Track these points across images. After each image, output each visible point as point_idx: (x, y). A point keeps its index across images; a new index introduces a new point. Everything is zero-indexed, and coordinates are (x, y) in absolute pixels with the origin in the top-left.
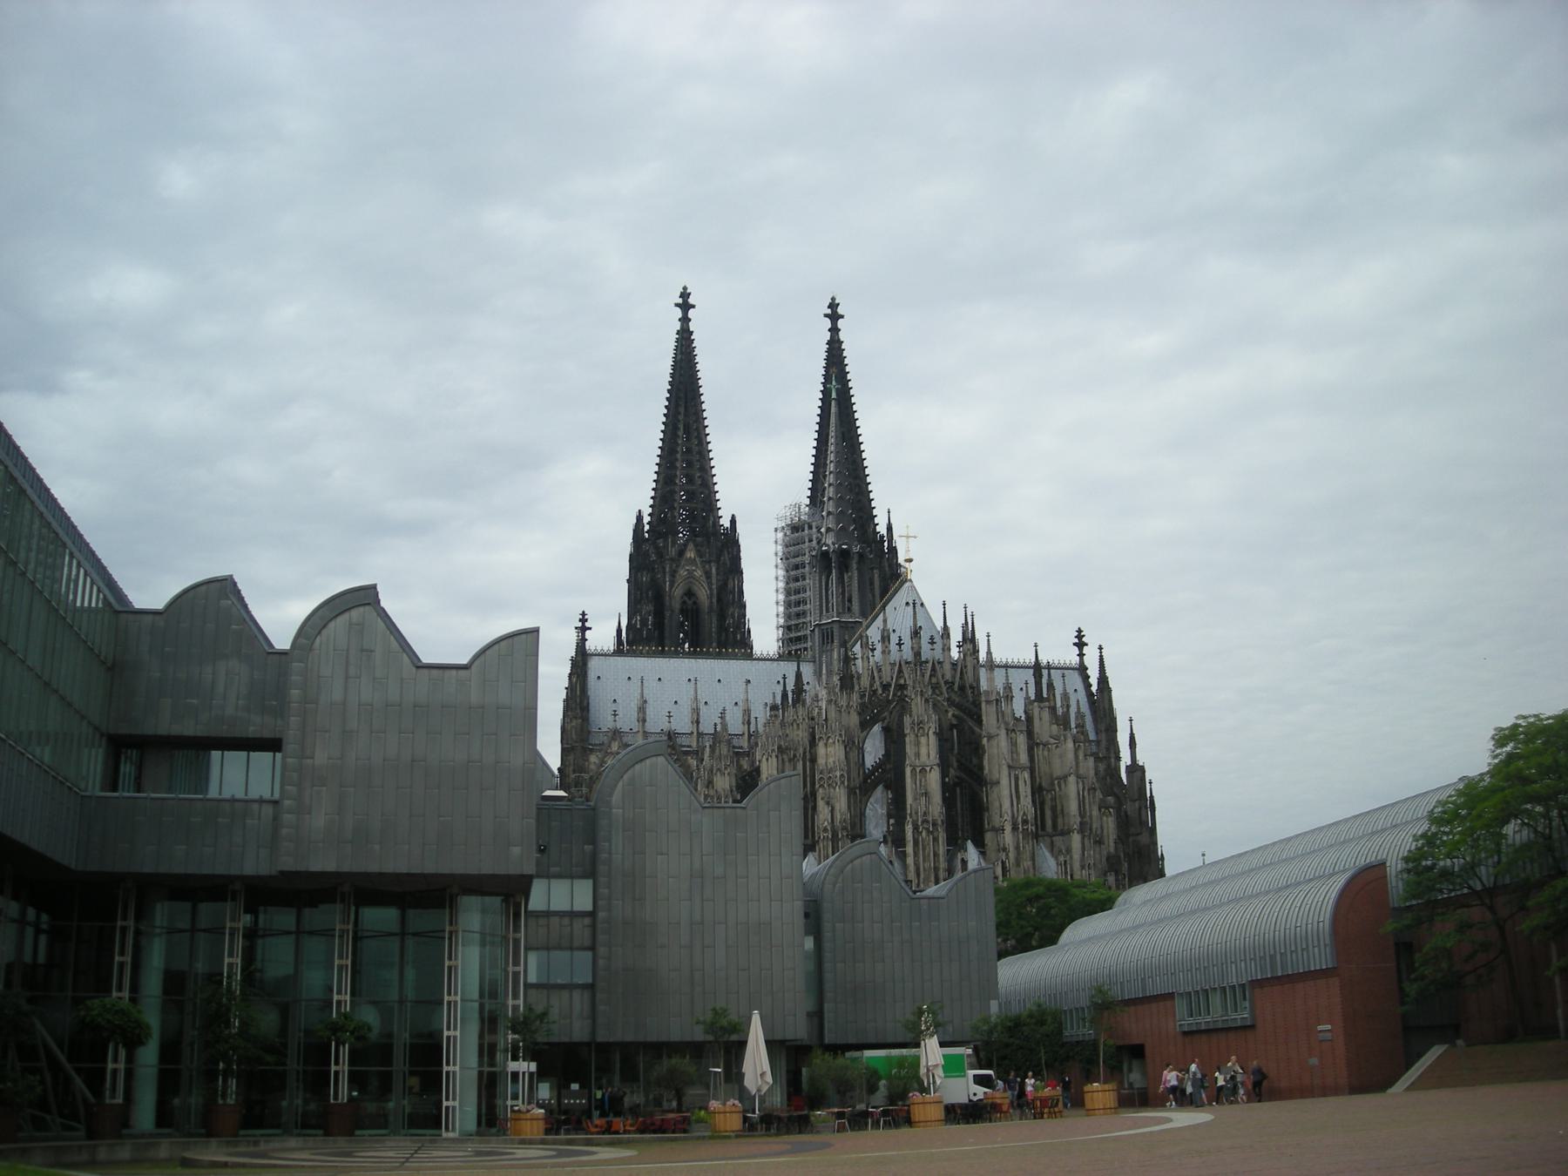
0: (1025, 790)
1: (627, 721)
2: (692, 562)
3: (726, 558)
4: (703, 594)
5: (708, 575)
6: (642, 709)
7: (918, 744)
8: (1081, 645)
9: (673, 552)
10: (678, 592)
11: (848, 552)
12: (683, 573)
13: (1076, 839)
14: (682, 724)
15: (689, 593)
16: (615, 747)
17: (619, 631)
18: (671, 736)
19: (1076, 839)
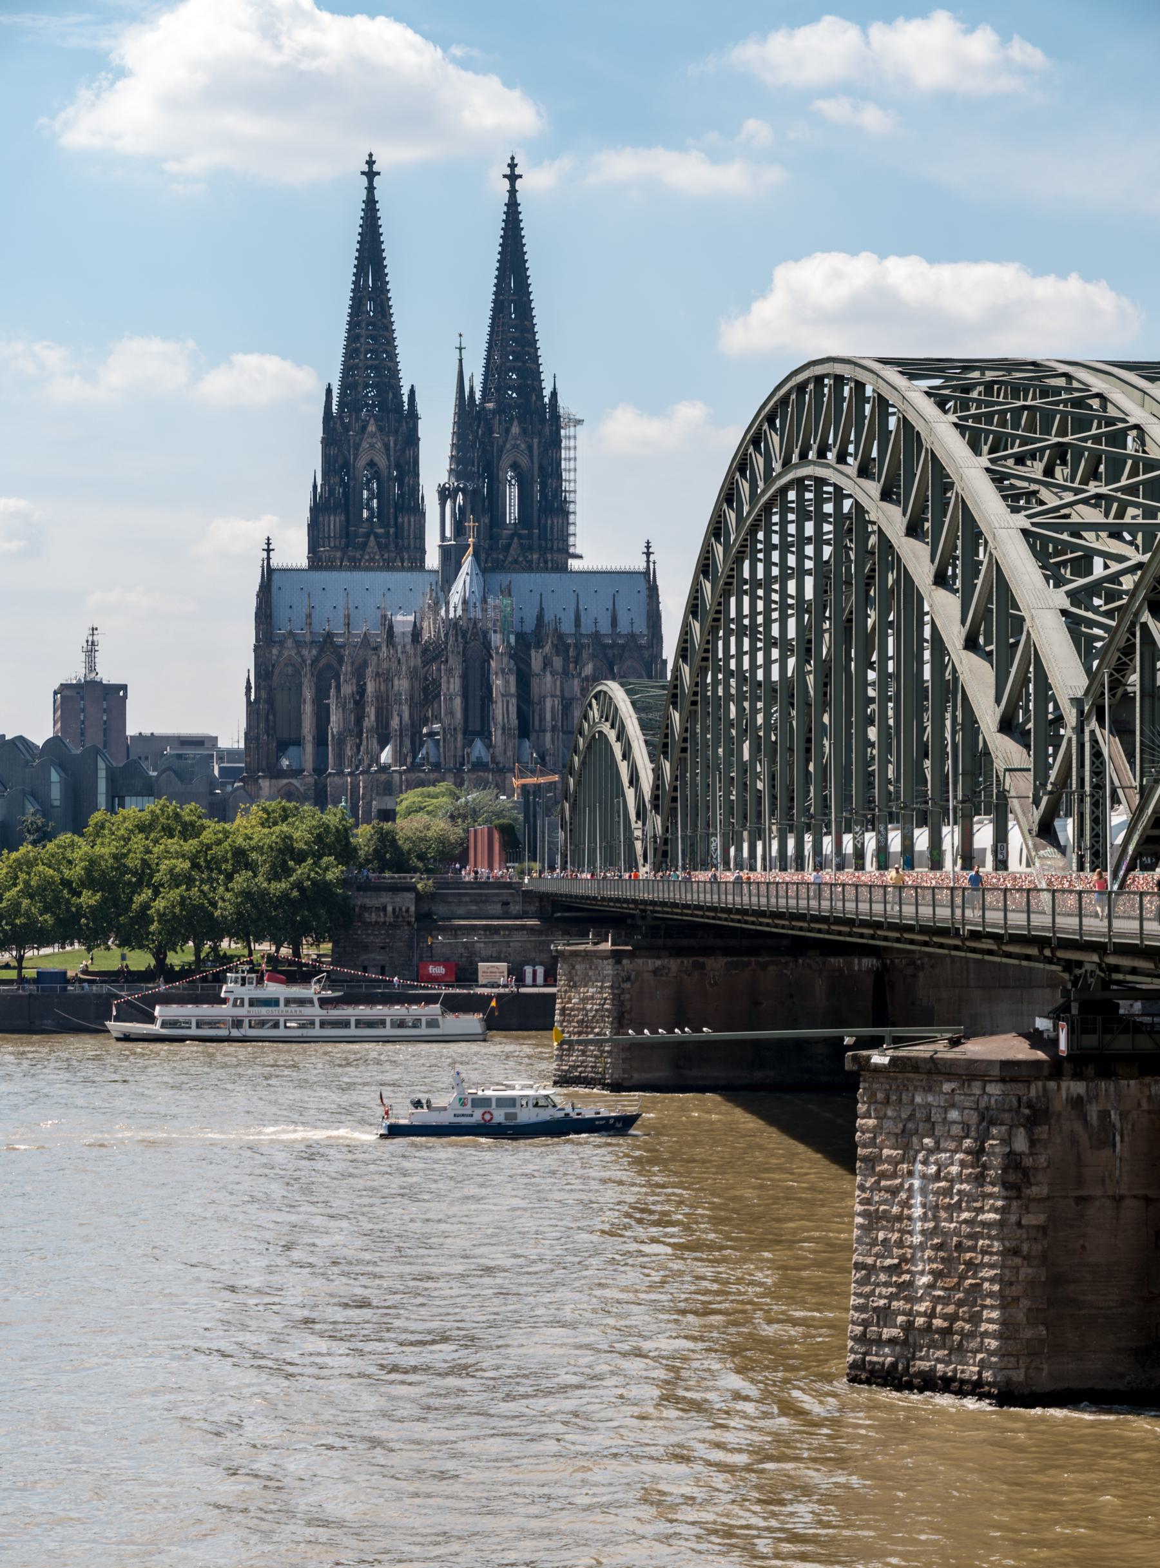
0: (513, 710)
2: (373, 435)
3: (404, 428)
4: (382, 462)
5: (387, 446)
6: (309, 616)
7: (449, 682)
8: (648, 554)
10: (362, 462)
12: (365, 445)
13: (548, 735)
15: (371, 464)
16: (290, 643)
17: (315, 487)
18: (329, 636)
19: (548, 735)
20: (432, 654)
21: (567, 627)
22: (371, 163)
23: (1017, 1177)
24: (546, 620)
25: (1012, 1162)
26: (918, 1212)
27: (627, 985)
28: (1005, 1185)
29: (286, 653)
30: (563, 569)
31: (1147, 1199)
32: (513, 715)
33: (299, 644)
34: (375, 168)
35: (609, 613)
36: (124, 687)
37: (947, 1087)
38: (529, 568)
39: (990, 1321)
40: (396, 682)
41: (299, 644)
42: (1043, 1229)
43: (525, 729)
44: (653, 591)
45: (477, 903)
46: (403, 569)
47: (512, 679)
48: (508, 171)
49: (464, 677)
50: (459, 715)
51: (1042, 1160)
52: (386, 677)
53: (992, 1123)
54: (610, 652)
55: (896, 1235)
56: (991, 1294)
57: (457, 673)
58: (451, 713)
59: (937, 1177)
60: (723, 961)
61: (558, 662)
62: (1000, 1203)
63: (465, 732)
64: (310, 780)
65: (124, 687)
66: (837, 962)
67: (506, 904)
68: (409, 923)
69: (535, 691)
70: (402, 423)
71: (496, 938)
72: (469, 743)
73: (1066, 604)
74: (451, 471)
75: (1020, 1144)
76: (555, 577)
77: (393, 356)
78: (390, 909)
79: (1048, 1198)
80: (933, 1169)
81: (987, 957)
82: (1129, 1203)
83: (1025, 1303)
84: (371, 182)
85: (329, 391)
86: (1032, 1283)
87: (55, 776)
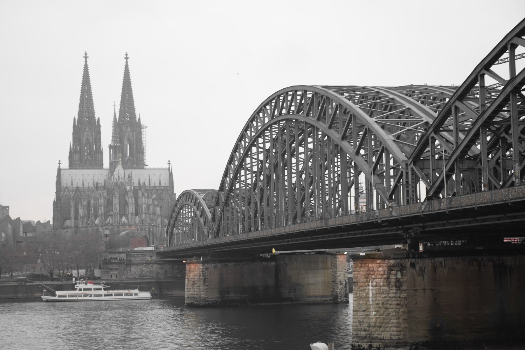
1: (69, 185)
4: (90, 139)
5: (92, 134)
6: (72, 182)
8: (169, 164)
9: (83, 129)
10: (84, 139)
11: (128, 125)
12: (85, 134)
13: (144, 215)
14: (80, 185)
15: (87, 139)
16: (66, 190)
17: (71, 146)
18: (78, 188)
19: (144, 215)
20: (110, 192)
21: (147, 185)
22: (86, 54)
23: (398, 284)
24: (141, 183)
25: (397, 281)
26: (371, 295)
27: (206, 271)
28: (396, 286)
29: (65, 193)
30: (143, 168)
31: (432, 290)
32: (134, 210)
33: (69, 191)
34: (87, 56)
35: (159, 181)
36: (8, 207)
37: (378, 261)
38: (134, 168)
39: (393, 323)
40: (100, 200)
41: (69, 191)
42: (405, 298)
43: (137, 214)
44: (171, 174)
45: (142, 256)
46: (97, 169)
47: (133, 199)
48: (125, 56)
49: (119, 199)
50: (118, 209)
51: (405, 279)
52: (96, 199)
53: (392, 270)
54: (159, 192)
55: (365, 302)
56: (393, 316)
57: (118, 197)
58: (116, 209)
59: (376, 286)
60: (233, 264)
61: (146, 194)
62: (394, 291)
63: (120, 214)
64: (73, 230)
65: (8, 207)
66: (265, 263)
67: (151, 256)
68: (124, 263)
69: (140, 202)
70: (96, 127)
71: (149, 266)
72: (121, 218)
73: (393, 139)
74: (112, 140)
75: (399, 276)
76: (143, 170)
77: (93, 109)
78: (118, 258)
79: (406, 290)
80: (374, 284)
81: (370, 235)
82: (427, 291)
83: (402, 317)
84: (86, 59)
85: (75, 119)
86: (404, 312)
87: (10, 226)
